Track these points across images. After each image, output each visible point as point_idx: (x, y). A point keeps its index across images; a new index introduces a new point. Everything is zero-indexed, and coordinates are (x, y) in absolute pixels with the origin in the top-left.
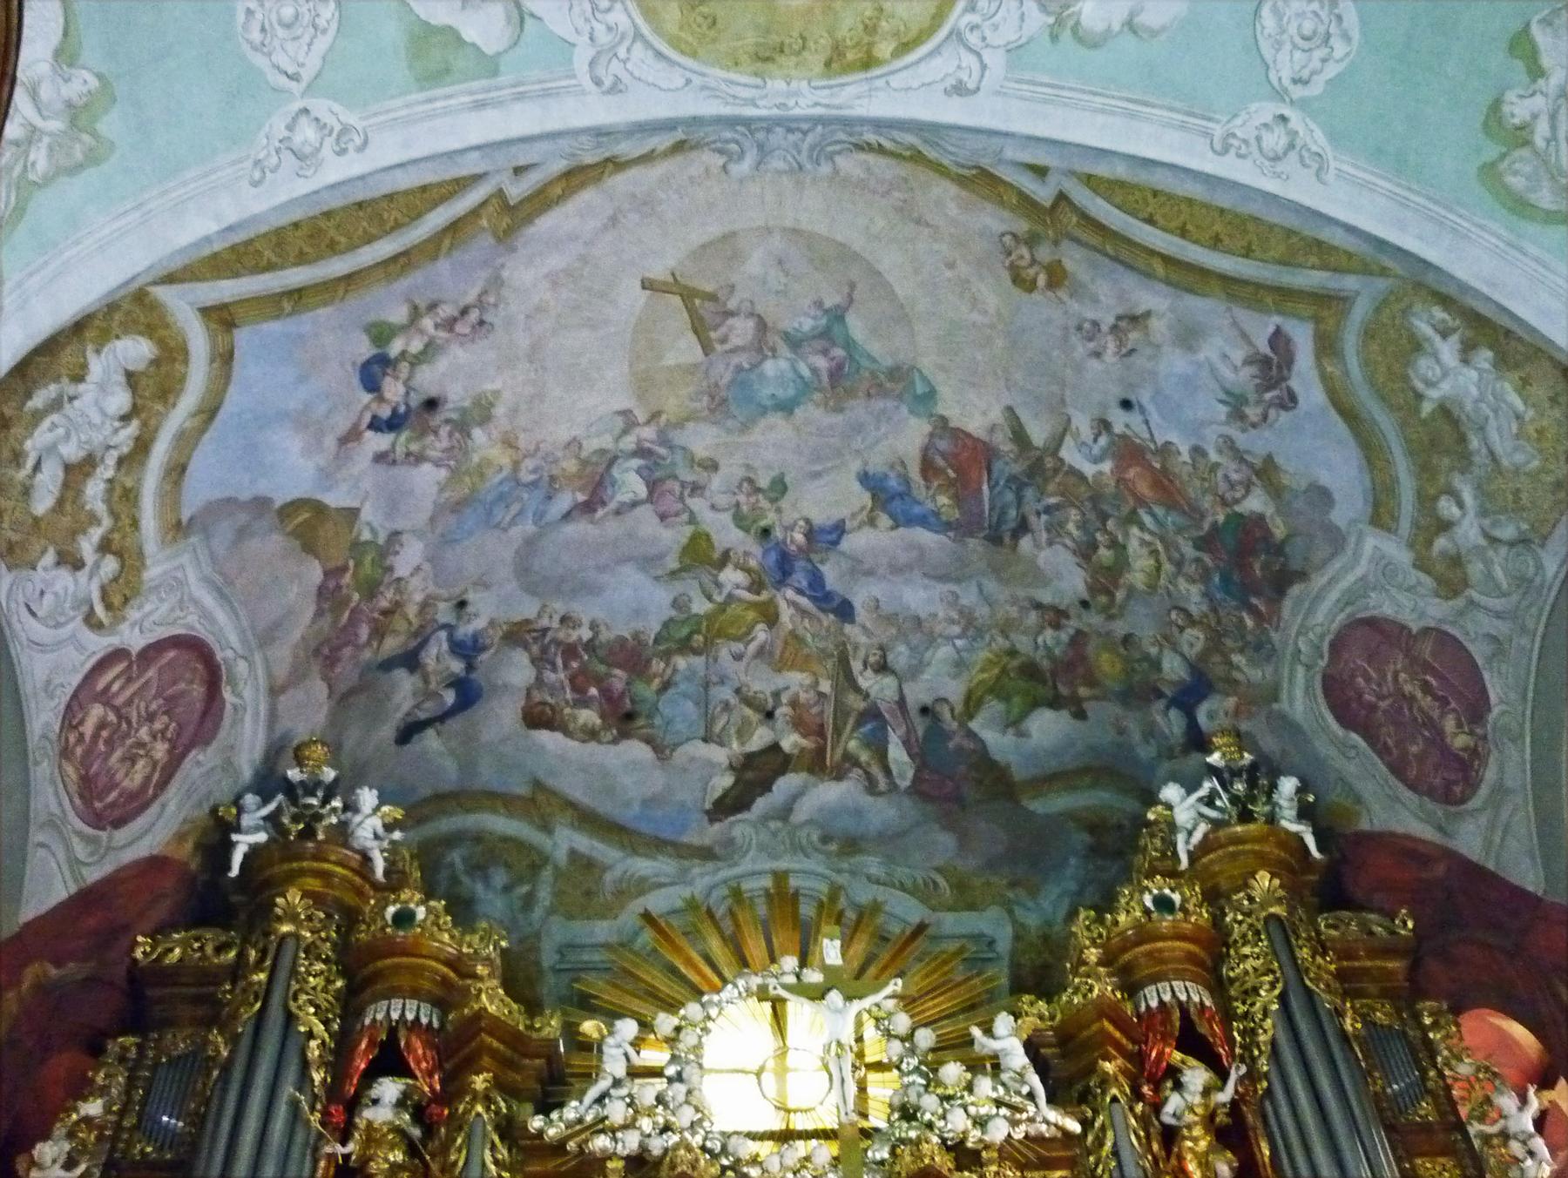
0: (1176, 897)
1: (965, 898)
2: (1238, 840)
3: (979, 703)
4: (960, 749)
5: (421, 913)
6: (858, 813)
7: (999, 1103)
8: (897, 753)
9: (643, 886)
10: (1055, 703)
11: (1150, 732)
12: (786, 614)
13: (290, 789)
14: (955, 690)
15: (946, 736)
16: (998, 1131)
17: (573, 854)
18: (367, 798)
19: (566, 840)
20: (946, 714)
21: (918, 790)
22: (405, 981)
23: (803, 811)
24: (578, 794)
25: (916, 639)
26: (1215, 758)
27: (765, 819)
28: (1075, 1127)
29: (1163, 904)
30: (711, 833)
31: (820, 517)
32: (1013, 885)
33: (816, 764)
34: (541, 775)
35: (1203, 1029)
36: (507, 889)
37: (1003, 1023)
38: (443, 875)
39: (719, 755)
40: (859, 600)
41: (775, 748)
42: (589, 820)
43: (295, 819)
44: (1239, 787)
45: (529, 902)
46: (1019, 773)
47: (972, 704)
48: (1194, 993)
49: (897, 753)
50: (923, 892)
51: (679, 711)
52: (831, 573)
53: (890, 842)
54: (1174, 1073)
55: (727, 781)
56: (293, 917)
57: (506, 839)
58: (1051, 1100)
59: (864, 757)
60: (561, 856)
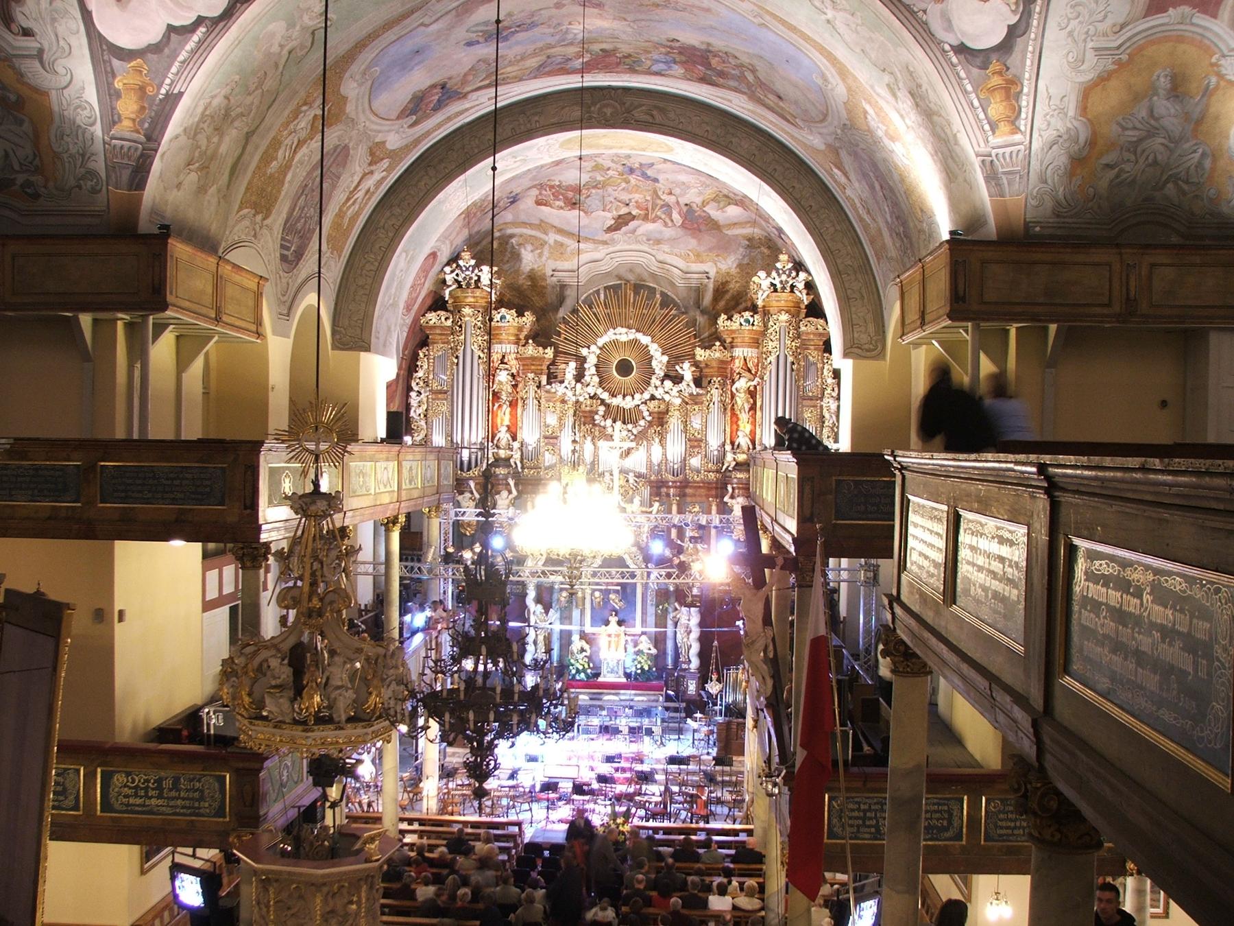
0: (751, 320)
1: (699, 258)
3: (708, 203)
4: (700, 216)
6: (661, 232)
8: (675, 216)
10: (736, 205)
12: (633, 181)
14: (699, 200)
15: (696, 212)
17: (556, 241)
20: (694, 206)
21: (683, 226)
23: (640, 231)
24: (556, 224)
25: (683, 187)
26: (779, 265)
27: (626, 233)
30: (607, 236)
31: (644, 162)
32: (717, 256)
33: (645, 218)
34: (543, 218)
35: (750, 365)
39: (609, 215)
40: (660, 178)
41: (630, 213)
42: (560, 231)
43: (465, 279)
45: (540, 255)
46: (721, 223)
47: (704, 204)
49: (675, 216)
50: (685, 257)
51: (593, 202)
52: (649, 173)
53: (672, 241)
55: (613, 222)
57: (530, 236)
59: (663, 216)
60: (551, 242)
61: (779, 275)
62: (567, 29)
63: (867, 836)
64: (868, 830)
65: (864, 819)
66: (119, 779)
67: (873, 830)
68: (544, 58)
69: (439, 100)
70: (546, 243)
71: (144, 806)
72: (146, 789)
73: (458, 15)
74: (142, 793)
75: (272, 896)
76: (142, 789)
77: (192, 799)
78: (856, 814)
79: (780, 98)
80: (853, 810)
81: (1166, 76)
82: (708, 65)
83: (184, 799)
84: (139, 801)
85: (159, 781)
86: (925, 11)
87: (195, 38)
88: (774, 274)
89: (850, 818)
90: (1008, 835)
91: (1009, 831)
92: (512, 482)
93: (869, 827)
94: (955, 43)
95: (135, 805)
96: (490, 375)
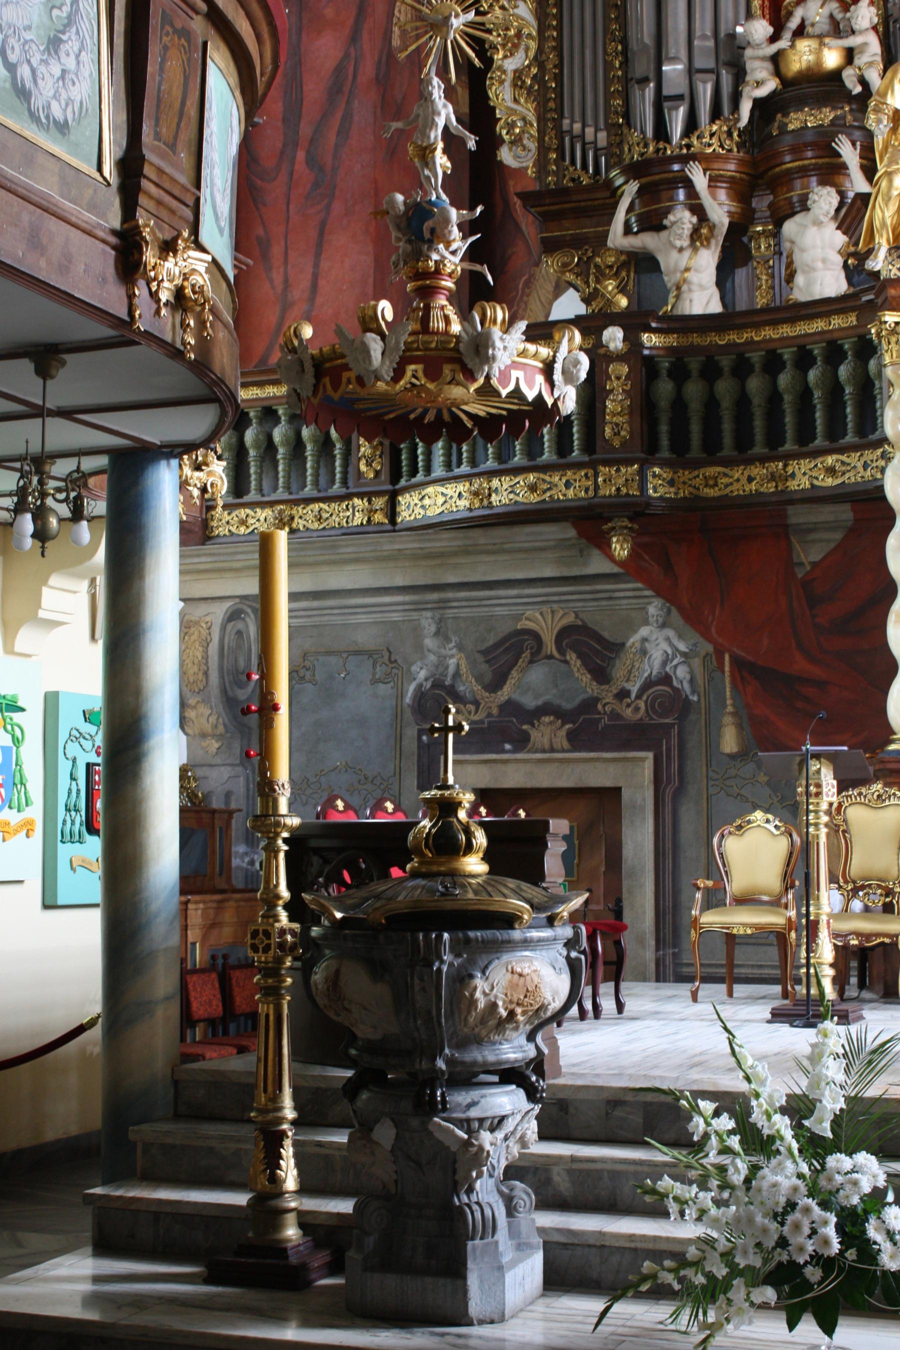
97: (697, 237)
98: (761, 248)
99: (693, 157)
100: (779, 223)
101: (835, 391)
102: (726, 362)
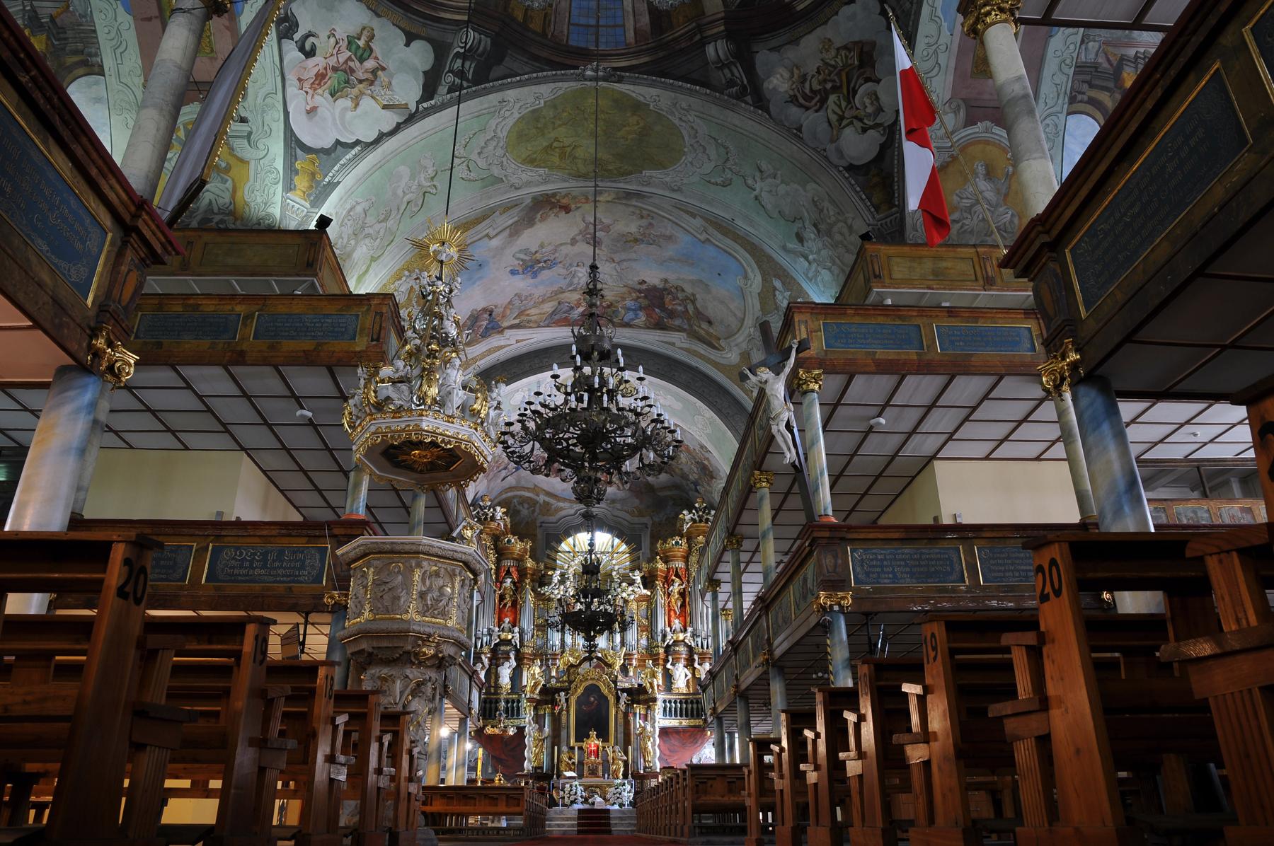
1: (641, 514)
2: (698, 527)
5: (513, 540)
6: (615, 494)
7: (633, 591)
9: (562, 509)
11: (687, 485)
13: (481, 507)
16: (632, 597)
18: (498, 508)
19: (542, 498)
22: (510, 556)
24: (545, 489)
26: (697, 505)
28: (649, 593)
29: (677, 543)
35: (680, 573)
36: (528, 509)
37: (637, 573)
38: (513, 505)
44: (701, 513)
45: (533, 511)
48: (680, 564)
50: (632, 514)
53: (623, 501)
54: (673, 581)
56: (485, 540)
58: (645, 587)
60: (541, 502)
61: (697, 512)
62: (575, 271)
63: (886, 581)
64: (886, 576)
65: (882, 566)
66: (227, 554)
67: (891, 576)
68: (555, 303)
69: (486, 328)
70: (537, 502)
71: (248, 575)
72: (251, 562)
73: (511, 235)
74: (248, 564)
75: (371, 578)
76: (248, 561)
77: (294, 568)
78: (874, 563)
79: (710, 322)
80: (872, 560)
81: (982, 166)
82: (662, 306)
83: (285, 568)
84: (243, 571)
85: (265, 554)
86: (825, 150)
87: (353, 152)
88: (694, 511)
89: (870, 566)
90: (1001, 577)
91: (1002, 574)
92: (512, 656)
93: (889, 573)
94: (846, 164)
95: (240, 575)
96: (500, 581)
97: (482, 669)
98: (494, 671)
99: (483, 653)
100: (498, 667)
101: (513, 708)
102: (494, 701)
